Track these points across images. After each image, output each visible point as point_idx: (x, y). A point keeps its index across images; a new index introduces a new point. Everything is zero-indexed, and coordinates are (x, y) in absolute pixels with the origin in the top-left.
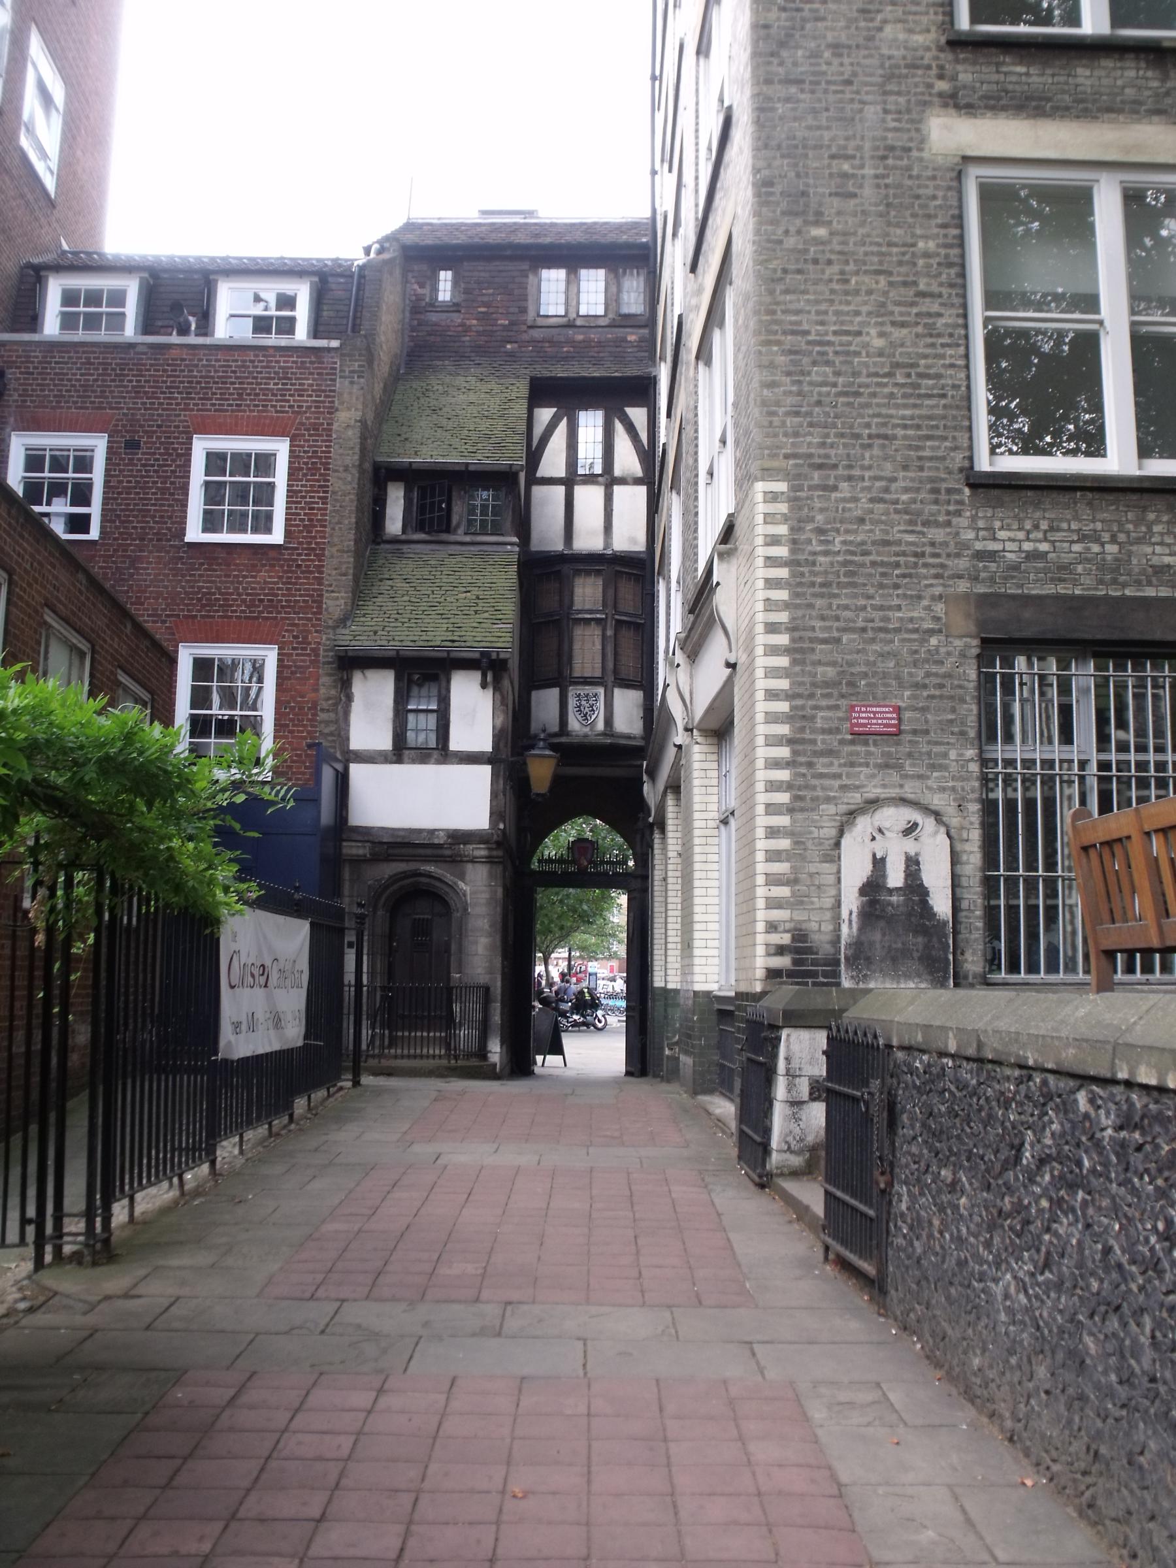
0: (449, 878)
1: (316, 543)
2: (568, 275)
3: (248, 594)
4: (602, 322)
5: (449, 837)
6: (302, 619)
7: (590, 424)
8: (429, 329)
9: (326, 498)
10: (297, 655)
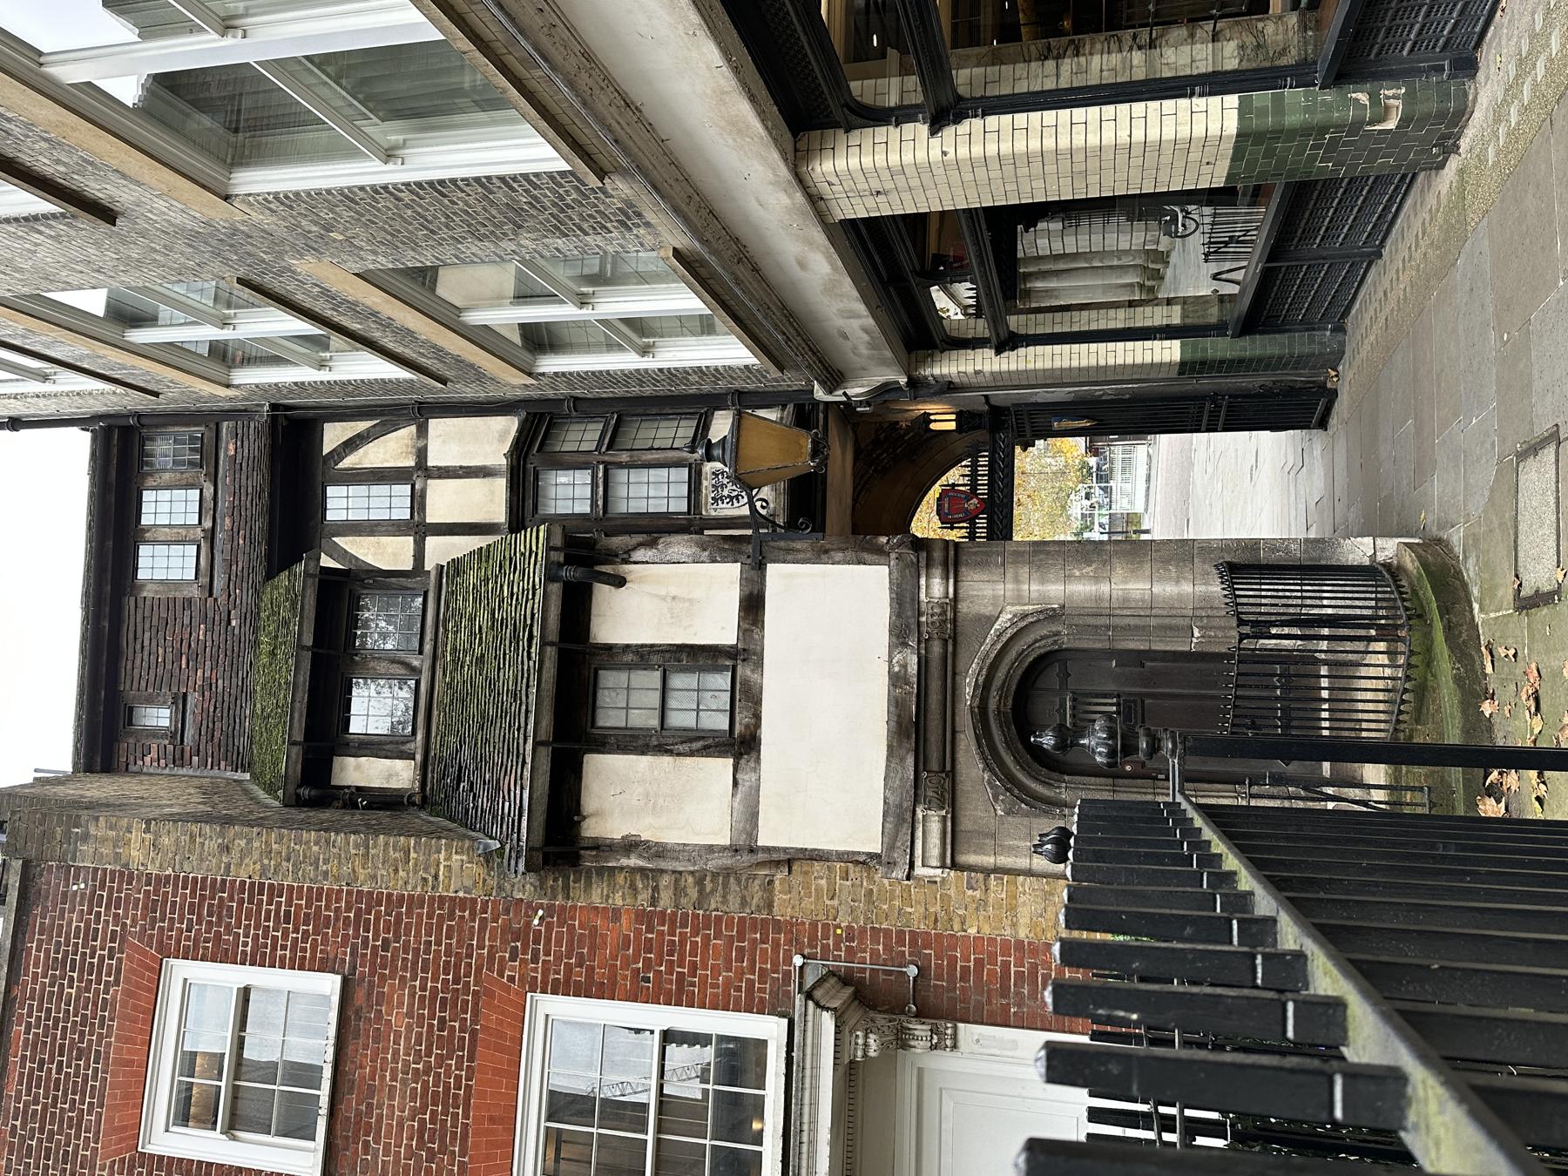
0: (989, 644)
1: (348, 910)
2: (146, 542)
3: (429, 1054)
4: (209, 490)
5: (905, 645)
6: (481, 940)
7: (341, 503)
8: (203, 738)
9: (271, 886)
10: (547, 953)
